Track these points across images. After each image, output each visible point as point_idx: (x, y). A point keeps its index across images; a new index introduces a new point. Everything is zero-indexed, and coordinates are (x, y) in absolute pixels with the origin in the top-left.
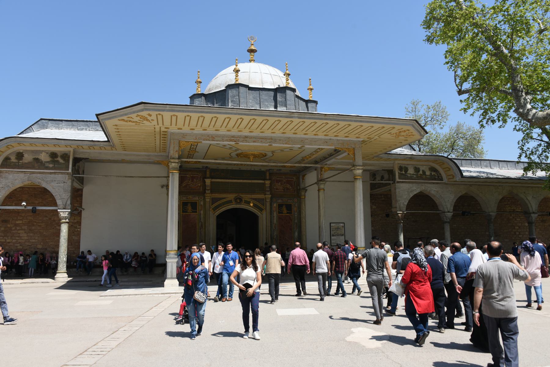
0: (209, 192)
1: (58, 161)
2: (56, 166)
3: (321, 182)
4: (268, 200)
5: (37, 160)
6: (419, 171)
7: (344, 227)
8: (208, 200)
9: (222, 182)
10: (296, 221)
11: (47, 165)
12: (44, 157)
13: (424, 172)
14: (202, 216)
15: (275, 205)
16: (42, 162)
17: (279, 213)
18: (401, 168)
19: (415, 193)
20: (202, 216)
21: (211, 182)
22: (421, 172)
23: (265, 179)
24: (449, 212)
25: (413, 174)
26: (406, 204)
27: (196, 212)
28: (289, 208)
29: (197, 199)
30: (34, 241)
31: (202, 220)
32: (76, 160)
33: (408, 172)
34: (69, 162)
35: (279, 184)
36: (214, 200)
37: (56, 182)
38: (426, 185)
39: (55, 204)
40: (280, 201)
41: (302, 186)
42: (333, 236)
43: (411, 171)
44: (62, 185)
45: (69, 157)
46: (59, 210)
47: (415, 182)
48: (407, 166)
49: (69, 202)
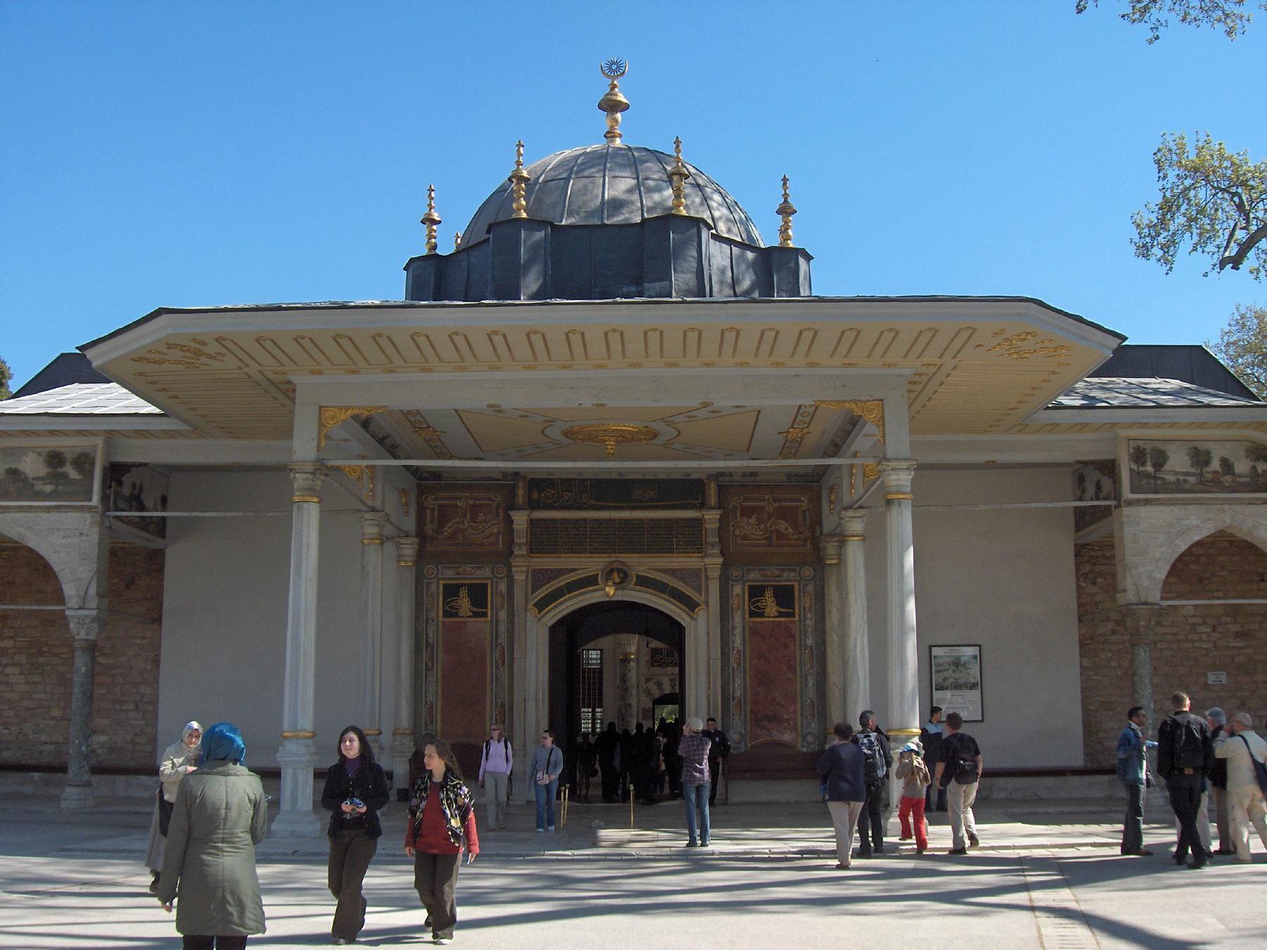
1: (65, 476)
2: (60, 488)
3: (851, 513)
4: (714, 573)
5: (14, 473)
6: (1207, 463)
7: (980, 658)
8: (519, 577)
9: (564, 520)
10: (810, 641)
11: (39, 486)
12: (32, 466)
13: (1227, 465)
14: (503, 628)
15: (737, 589)
16: (26, 480)
17: (752, 614)
18: (1139, 456)
19: (1196, 538)
20: (503, 628)
21: (533, 523)
22: (1215, 465)
23: (702, 506)
25: (1187, 474)
26: (1161, 575)
27: (485, 615)
28: (785, 596)
29: (488, 574)
30: (42, 696)
31: (503, 639)
32: (115, 472)
33: (1167, 467)
34: (92, 478)
36: (539, 578)
37: (62, 534)
38: (1238, 508)
39: (61, 600)
41: (829, 523)
42: (940, 688)
43: (1178, 462)
44: (77, 541)
45: (93, 464)
46: (67, 613)
47: (1194, 502)
48: (1160, 446)
49: (93, 590)
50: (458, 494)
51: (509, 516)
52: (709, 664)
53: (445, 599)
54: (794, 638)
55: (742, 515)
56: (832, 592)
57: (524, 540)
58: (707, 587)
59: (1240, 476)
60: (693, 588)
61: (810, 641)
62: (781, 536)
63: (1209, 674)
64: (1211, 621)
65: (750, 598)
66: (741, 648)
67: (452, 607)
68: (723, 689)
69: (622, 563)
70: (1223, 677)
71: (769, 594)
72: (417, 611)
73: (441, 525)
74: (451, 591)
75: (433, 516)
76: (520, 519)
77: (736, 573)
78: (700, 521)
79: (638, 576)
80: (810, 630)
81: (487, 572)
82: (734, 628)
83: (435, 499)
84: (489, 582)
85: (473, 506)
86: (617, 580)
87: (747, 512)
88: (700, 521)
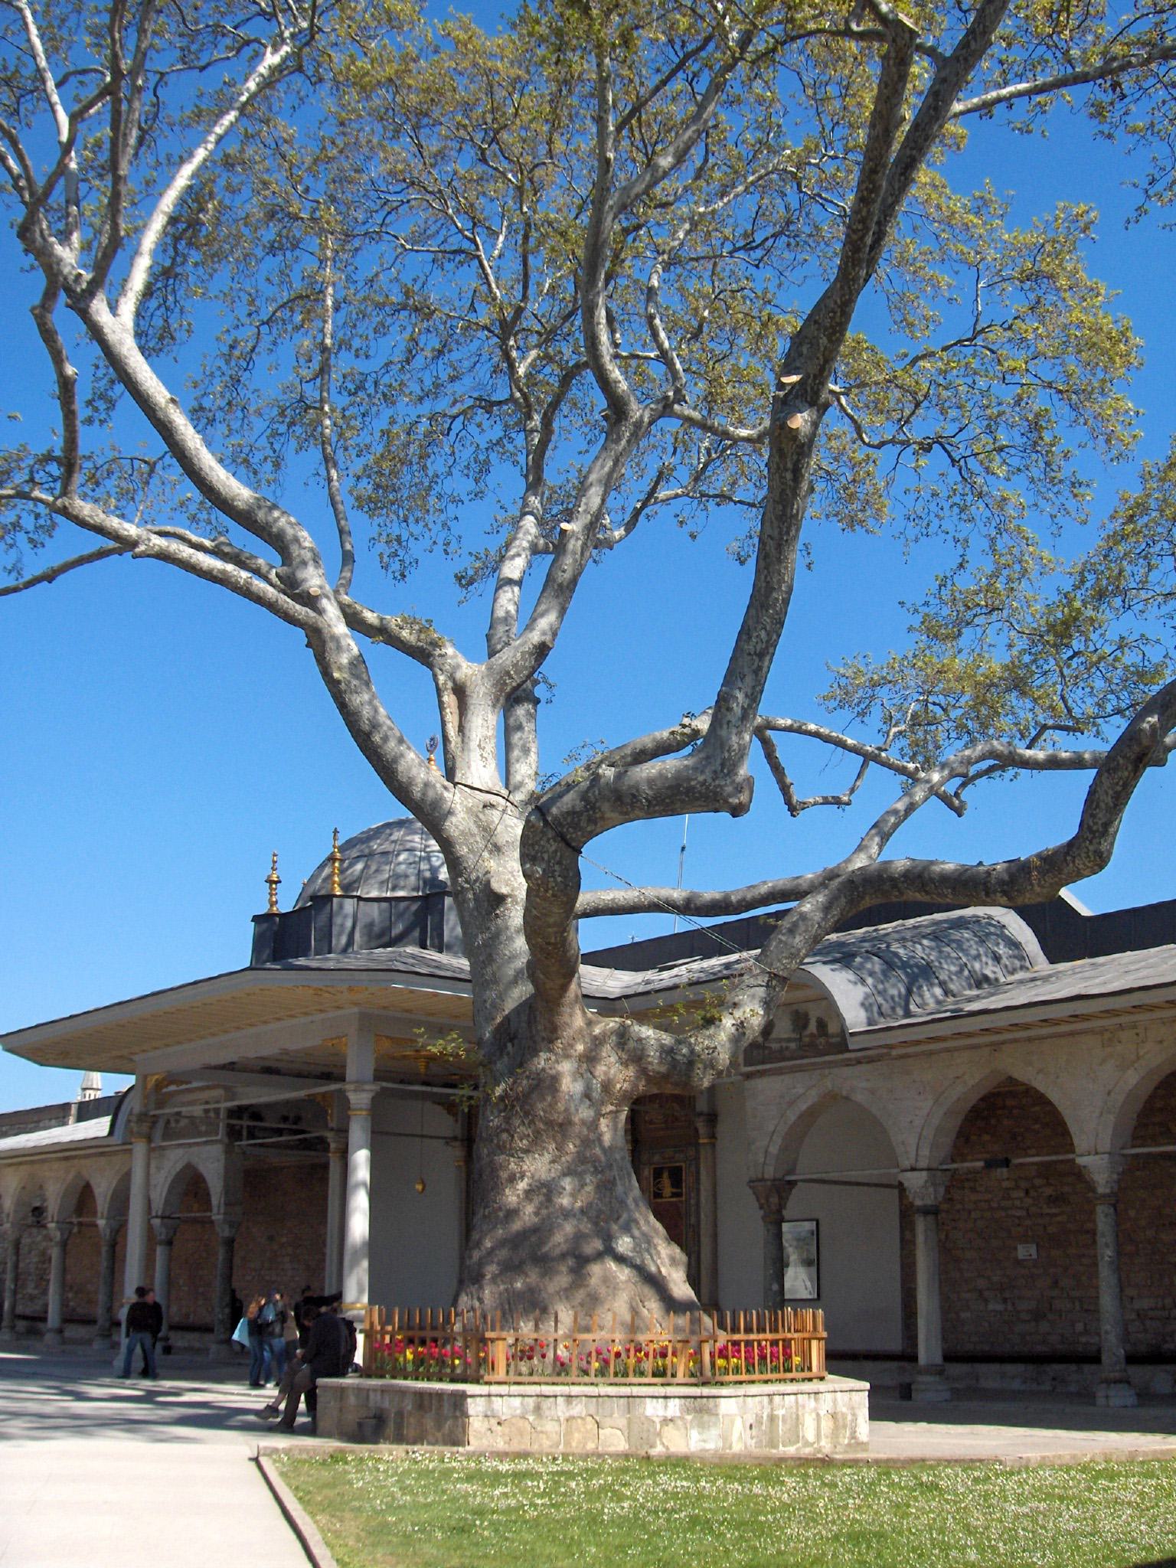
6: (805, 1026)
24: (913, 1169)
25: (789, 1040)
59: (833, 1036)
63: (1020, 1247)
64: (1023, 1184)
70: (1033, 1250)
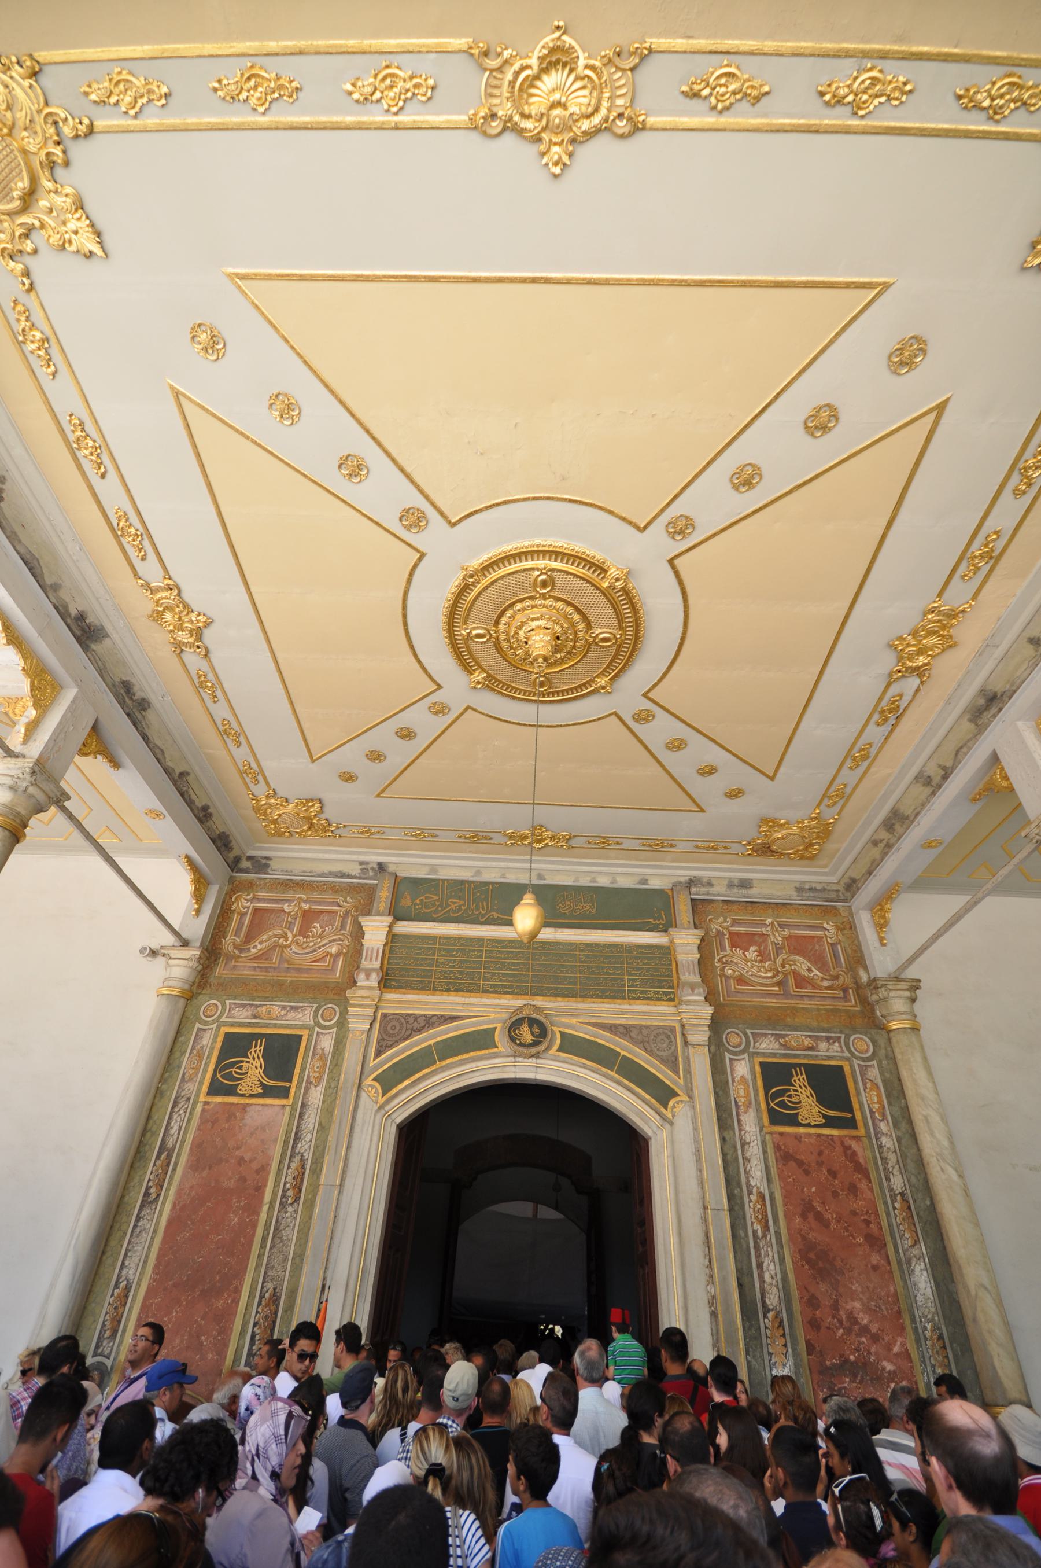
0: (374, 980)
4: (700, 1036)
8: (358, 1025)
10: (898, 1182)
14: (311, 1120)
17: (776, 1118)
21: (392, 938)
27: (284, 1093)
31: (307, 1147)
35: (752, 953)
36: (393, 1029)
40: (768, 1046)
41: (881, 962)
50: (289, 895)
51: (361, 927)
52: (705, 1220)
53: (221, 1058)
54: (861, 1170)
55: (733, 945)
56: (915, 1080)
57: (377, 965)
58: (687, 1060)
60: (663, 1061)
61: (898, 1182)
62: (801, 981)
65: (767, 1089)
66: (764, 1189)
67: (229, 1077)
68: (741, 1286)
69: (538, 1009)
71: (800, 1080)
72: (162, 1080)
73: (249, 939)
74: (235, 1046)
75: (240, 924)
76: (376, 931)
77: (733, 1038)
78: (666, 952)
79: (562, 1034)
80: (892, 1158)
81: (306, 1017)
82: (744, 1144)
83: (251, 901)
84: (305, 1033)
85: (305, 912)
86: (529, 1038)
87: (740, 941)
88: (666, 952)
